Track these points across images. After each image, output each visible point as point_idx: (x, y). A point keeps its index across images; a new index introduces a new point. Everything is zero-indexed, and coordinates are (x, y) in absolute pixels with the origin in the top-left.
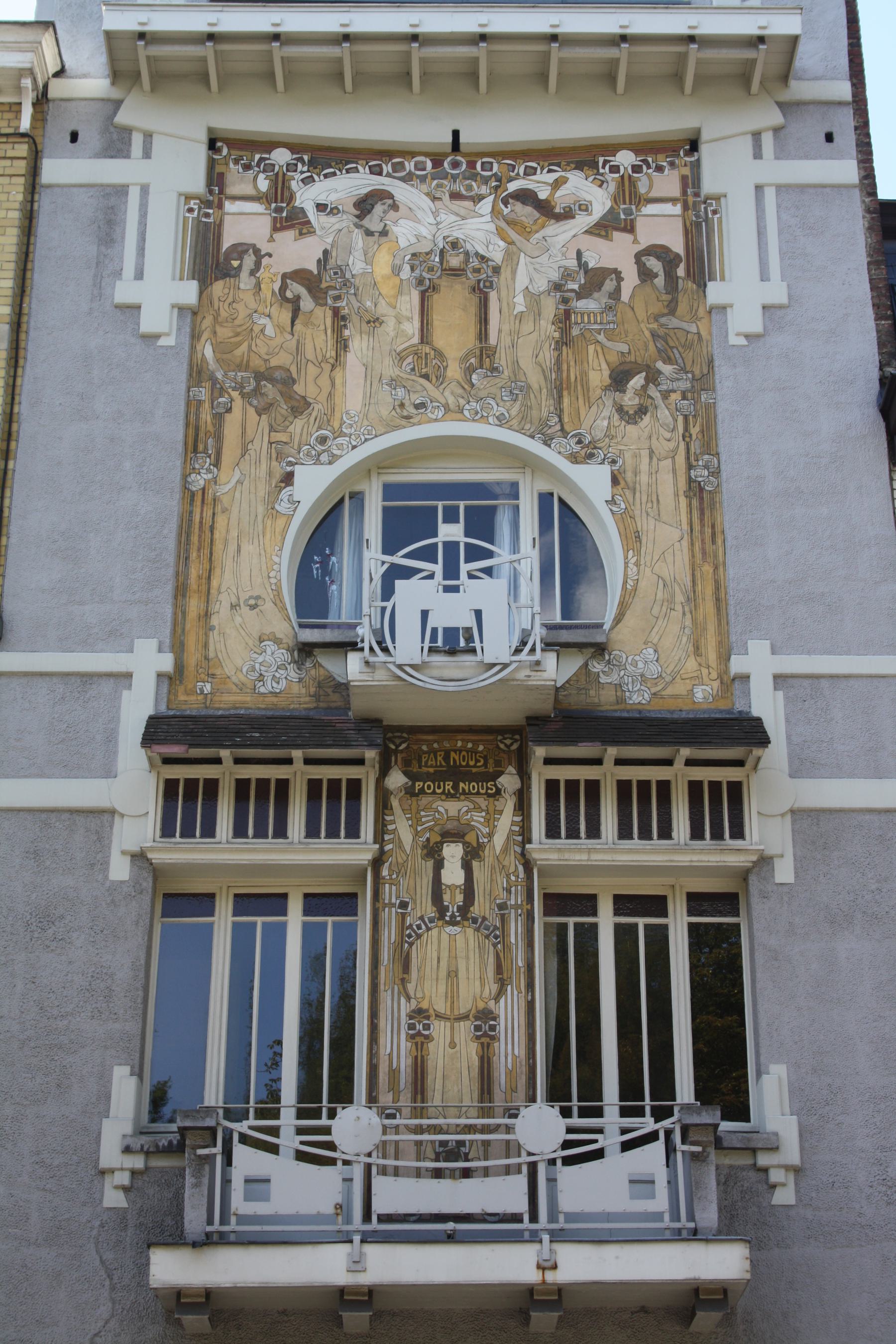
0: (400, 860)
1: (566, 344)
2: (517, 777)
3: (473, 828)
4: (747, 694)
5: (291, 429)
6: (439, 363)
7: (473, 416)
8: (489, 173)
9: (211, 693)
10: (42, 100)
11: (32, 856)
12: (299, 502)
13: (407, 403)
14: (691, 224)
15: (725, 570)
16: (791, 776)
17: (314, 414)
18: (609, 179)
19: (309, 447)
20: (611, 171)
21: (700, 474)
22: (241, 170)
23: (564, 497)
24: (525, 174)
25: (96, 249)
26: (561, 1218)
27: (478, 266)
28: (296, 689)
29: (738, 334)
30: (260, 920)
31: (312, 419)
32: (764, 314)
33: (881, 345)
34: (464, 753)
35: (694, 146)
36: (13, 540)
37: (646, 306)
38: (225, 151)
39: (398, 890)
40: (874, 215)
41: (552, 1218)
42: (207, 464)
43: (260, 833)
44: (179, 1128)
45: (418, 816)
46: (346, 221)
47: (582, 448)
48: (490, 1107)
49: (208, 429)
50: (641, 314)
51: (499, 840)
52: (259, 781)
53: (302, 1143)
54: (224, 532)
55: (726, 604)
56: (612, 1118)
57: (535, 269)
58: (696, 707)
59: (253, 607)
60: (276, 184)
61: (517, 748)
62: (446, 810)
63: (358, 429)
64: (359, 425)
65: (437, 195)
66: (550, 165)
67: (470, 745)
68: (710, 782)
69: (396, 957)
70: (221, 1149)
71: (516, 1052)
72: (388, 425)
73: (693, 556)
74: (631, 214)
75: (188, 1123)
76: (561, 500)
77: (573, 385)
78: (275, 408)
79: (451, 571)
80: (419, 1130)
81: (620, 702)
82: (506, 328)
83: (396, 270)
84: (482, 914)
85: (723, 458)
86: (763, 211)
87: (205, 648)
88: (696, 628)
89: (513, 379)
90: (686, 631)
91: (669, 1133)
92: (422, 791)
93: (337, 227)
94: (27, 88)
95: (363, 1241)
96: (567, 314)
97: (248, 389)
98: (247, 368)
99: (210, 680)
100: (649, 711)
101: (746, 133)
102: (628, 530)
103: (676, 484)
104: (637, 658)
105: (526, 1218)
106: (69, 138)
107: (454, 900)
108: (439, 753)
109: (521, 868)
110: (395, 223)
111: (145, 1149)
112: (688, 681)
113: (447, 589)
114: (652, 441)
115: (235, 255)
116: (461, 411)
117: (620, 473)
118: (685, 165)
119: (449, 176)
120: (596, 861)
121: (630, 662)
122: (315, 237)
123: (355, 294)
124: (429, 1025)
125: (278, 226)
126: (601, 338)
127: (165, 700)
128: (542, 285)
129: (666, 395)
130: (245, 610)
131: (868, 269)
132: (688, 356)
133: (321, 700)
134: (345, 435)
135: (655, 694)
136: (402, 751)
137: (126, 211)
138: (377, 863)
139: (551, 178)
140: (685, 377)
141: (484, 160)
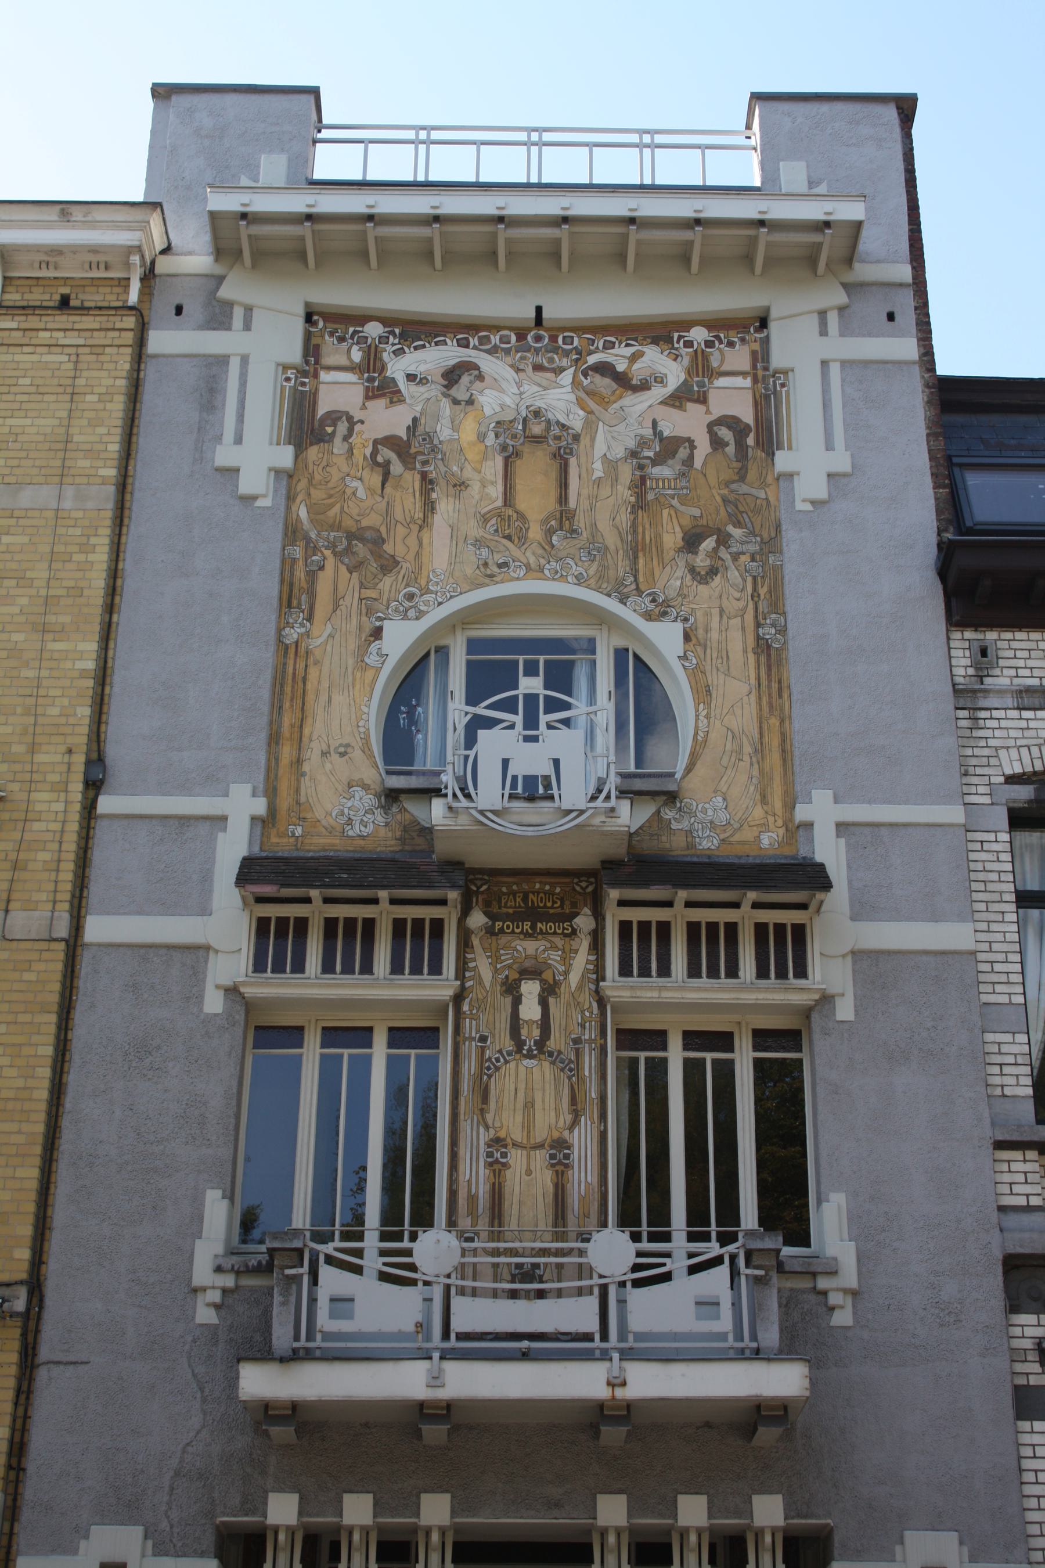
0: (480, 996)
1: (642, 508)
2: (592, 917)
3: (550, 966)
4: (811, 841)
5: (380, 586)
8: (570, 347)
9: (302, 836)
10: (149, 275)
11: (131, 989)
13: (490, 562)
15: (790, 723)
16: (852, 919)
17: (403, 572)
18: (683, 354)
20: (685, 346)
21: (768, 632)
22: (335, 342)
23: (638, 652)
24: (604, 347)
26: (631, 1337)
27: (559, 434)
28: (383, 832)
29: (804, 501)
30: (346, 1052)
31: (401, 577)
32: (829, 482)
33: (939, 512)
34: (542, 895)
35: (763, 323)
36: (116, 689)
38: (321, 324)
39: (478, 1026)
41: (622, 1337)
42: (301, 619)
43: (348, 969)
44: (268, 1249)
46: (434, 390)
47: (656, 606)
48: (564, 1232)
49: (302, 585)
50: (713, 481)
51: (574, 978)
53: (385, 1264)
54: (316, 683)
55: (792, 756)
56: (679, 1242)
57: (612, 437)
59: (342, 755)
60: (369, 355)
62: (525, 949)
63: (444, 587)
64: (445, 583)
65: (521, 367)
67: (547, 887)
68: (775, 925)
69: (476, 1088)
70: (307, 1269)
71: (589, 1180)
72: (472, 583)
73: (761, 710)
74: (704, 386)
75: (276, 1244)
76: (636, 656)
77: (648, 546)
79: (531, 722)
80: (496, 1253)
81: (690, 846)
82: (585, 492)
83: (481, 437)
84: (558, 1048)
85: (790, 617)
86: (829, 384)
88: (763, 778)
89: (591, 540)
90: (753, 780)
91: (733, 1258)
92: (502, 931)
93: (426, 396)
95: (441, 1358)
96: (643, 479)
97: (340, 548)
98: (339, 528)
99: (301, 823)
100: (718, 856)
101: (813, 312)
102: (699, 684)
103: (744, 641)
104: (707, 806)
105: (597, 1337)
106: (174, 312)
107: (531, 1035)
109: (595, 1005)
110: (481, 392)
111: (236, 1268)
112: (755, 828)
113: (527, 739)
115: (329, 422)
116: (541, 570)
119: (533, 350)
120: (666, 998)
121: (700, 808)
122: (405, 405)
123: (442, 459)
124: (506, 1153)
125: (370, 395)
126: (675, 502)
127: (259, 842)
128: (619, 452)
129: (735, 557)
130: (335, 757)
131: (927, 440)
134: (432, 592)
135: (723, 840)
136: (483, 892)
137: (226, 380)
138: (458, 998)
139: (629, 351)
141: (566, 334)
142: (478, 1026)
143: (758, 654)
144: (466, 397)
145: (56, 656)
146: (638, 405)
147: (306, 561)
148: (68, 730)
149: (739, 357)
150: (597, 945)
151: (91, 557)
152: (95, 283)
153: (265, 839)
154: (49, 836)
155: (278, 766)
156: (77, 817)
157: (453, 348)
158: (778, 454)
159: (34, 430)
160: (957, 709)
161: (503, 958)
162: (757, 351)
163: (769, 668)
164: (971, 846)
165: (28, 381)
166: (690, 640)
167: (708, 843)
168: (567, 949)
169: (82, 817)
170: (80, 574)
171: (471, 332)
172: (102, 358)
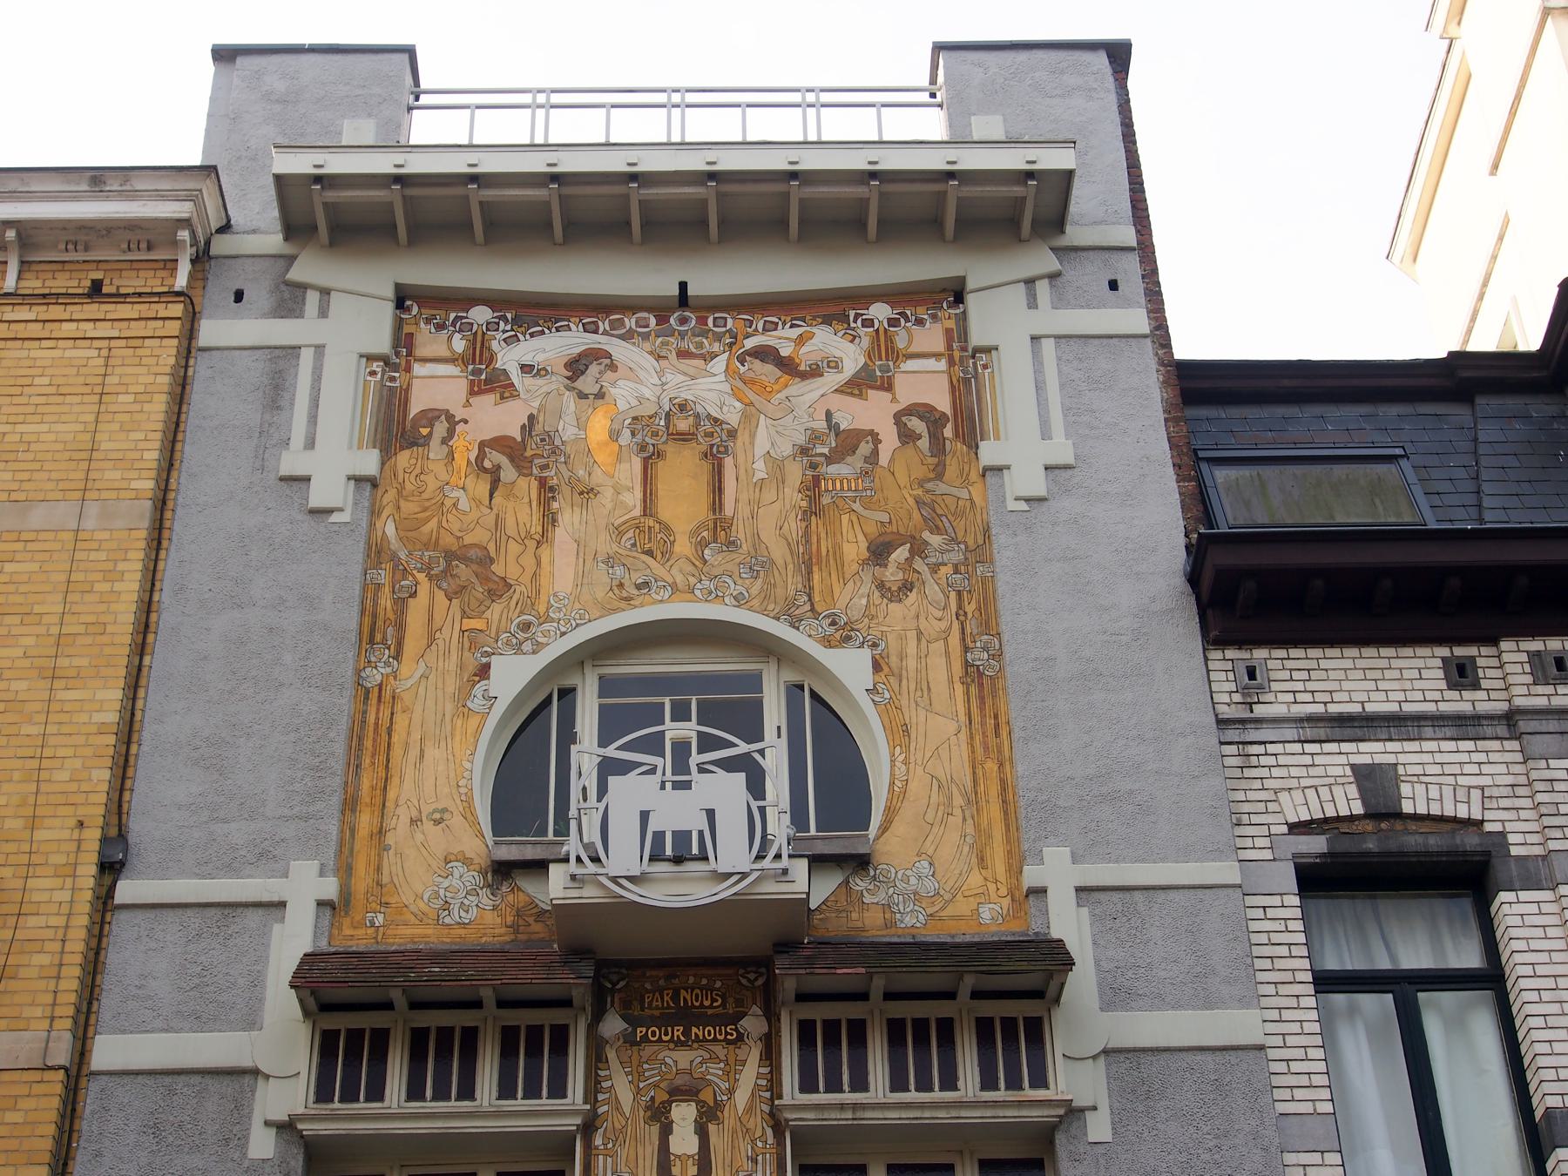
0: (617, 1126)
1: (816, 516)
3: (709, 1083)
5: (488, 614)
6: (665, 538)
7: (705, 596)
8: (724, 329)
9: (383, 926)
10: (202, 258)
12: (496, 698)
13: (626, 582)
14: (959, 381)
16: (1102, 1009)
18: (862, 334)
19: (509, 635)
21: (979, 657)
22: (433, 330)
25: (260, 416)
27: (711, 430)
35: (959, 298)
37: (909, 470)
38: (415, 310)
39: (615, 1164)
40: (1169, 368)
42: (386, 656)
45: (640, 1069)
46: (556, 382)
47: (837, 630)
50: (903, 479)
51: (742, 1097)
52: (440, 1030)
57: (777, 432)
58: (983, 928)
59: (437, 822)
61: (763, 985)
63: (568, 613)
64: (569, 608)
66: (796, 319)
67: (704, 981)
73: (973, 752)
76: (812, 691)
78: (468, 591)
82: (744, 497)
83: (614, 435)
85: (1005, 638)
86: (1042, 364)
87: (378, 872)
88: (980, 836)
89: (753, 553)
92: (645, 1038)
93: (545, 389)
94: (184, 241)
100: (925, 936)
101: (1019, 282)
102: (894, 723)
104: (909, 873)
108: (665, 992)
109: (769, 1131)
110: (613, 384)
112: (971, 899)
114: (920, 621)
115: (424, 422)
117: (883, 658)
118: (949, 318)
119: (676, 333)
121: (900, 877)
123: (565, 463)
125: (475, 390)
128: (787, 450)
129: (934, 569)
130: (428, 825)
131: (1166, 426)
132: (960, 525)
133: (520, 931)
134: (553, 620)
135: (931, 915)
137: (296, 375)
138: (589, 1127)
140: (957, 548)
141: (716, 315)
142: (615, 1164)
143: (968, 685)
144: (595, 389)
145: (67, 707)
146: (808, 394)
147: (394, 588)
148: (80, 799)
149: (930, 336)
150: (770, 1055)
151: (118, 586)
152: (135, 265)
153: (336, 932)
154: (50, 934)
155: (354, 839)
156: (87, 908)
157: (579, 334)
158: (983, 445)
159: (52, 437)
160: (1222, 743)
161: (646, 1074)
162: (952, 329)
163: (982, 699)
164: (1252, 913)
165: (46, 381)
166: (882, 670)
167: (912, 922)
168: (731, 1061)
169: (94, 909)
170: (103, 607)
171: (600, 316)
172: (140, 352)
